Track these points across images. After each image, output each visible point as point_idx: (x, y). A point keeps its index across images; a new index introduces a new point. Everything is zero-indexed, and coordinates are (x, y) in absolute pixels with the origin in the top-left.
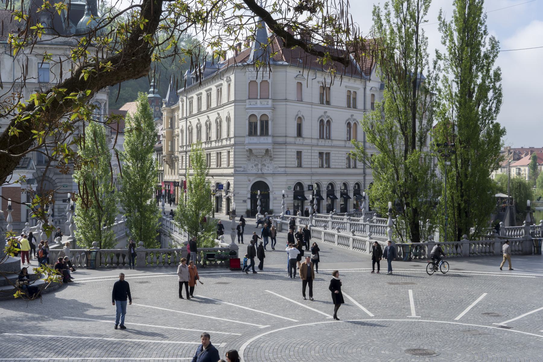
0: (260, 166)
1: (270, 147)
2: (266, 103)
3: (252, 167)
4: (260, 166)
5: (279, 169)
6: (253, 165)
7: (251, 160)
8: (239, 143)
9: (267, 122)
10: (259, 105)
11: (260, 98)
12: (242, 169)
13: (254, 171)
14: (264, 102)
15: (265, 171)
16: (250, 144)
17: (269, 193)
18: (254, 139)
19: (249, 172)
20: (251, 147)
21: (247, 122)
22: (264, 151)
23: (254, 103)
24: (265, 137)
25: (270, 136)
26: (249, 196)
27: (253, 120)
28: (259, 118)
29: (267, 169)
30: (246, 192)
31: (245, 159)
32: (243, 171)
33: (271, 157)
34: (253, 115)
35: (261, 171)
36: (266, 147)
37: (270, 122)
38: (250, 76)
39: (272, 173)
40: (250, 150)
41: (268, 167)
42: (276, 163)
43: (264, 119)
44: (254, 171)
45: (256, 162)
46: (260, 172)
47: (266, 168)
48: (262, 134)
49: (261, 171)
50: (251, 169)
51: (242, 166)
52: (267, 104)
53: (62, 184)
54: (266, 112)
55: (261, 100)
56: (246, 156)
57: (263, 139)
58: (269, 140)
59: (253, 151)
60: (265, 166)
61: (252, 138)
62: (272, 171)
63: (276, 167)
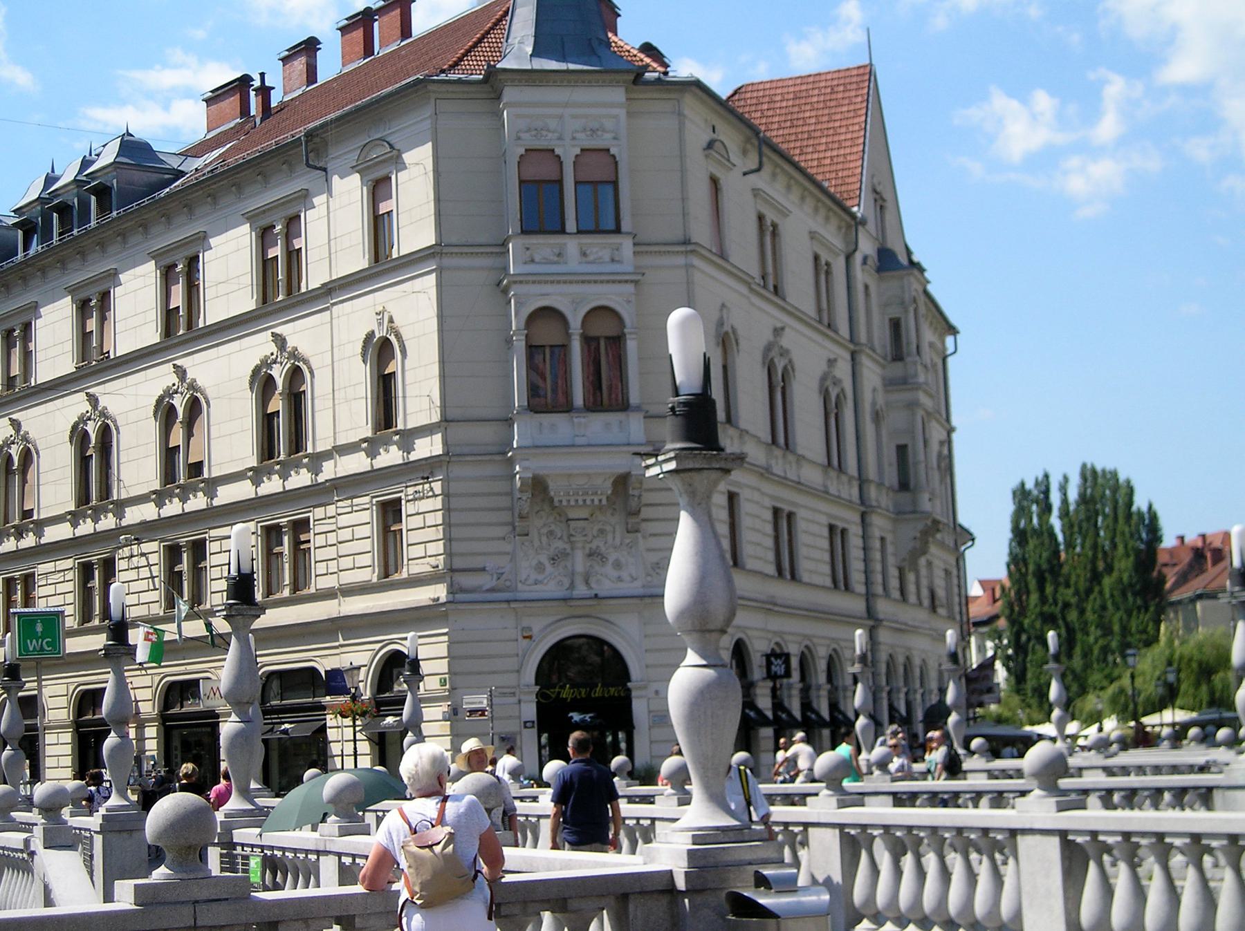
0: (579, 562)
2: (606, 254)
3: (540, 568)
4: (579, 562)
6: (544, 559)
7: (534, 533)
8: (466, 450)
9: (617, 341)
10: (573, 263)
11: (579, 232)
12: (485, 581)
14: (599, 246)
15: (605, 586)
17: (629, 690)
19: (525, 591)
24: (613, 418)
25: (638, 409)
26: (530, 711)
27: (548, 334)
29: (614, 574)
32: (492, 590)
34: (547, 313)
35: (587, 583)
37: (631, 346)
39: (640, 591)
41: (618, 565)
43: (603, 328)
44: (551, 588)
45: (560, 545)
46: (581, 590)
47: (609, 569)
48: (596, 404)
49: (587, 583)
50: (534, 576)
51: (490, 563)
52: (613, 260)
54: (612, 296)
55: (587, 240)
57: (598, 425)
59: (552, 486)
61: (547, 419)
62: (638, 584)
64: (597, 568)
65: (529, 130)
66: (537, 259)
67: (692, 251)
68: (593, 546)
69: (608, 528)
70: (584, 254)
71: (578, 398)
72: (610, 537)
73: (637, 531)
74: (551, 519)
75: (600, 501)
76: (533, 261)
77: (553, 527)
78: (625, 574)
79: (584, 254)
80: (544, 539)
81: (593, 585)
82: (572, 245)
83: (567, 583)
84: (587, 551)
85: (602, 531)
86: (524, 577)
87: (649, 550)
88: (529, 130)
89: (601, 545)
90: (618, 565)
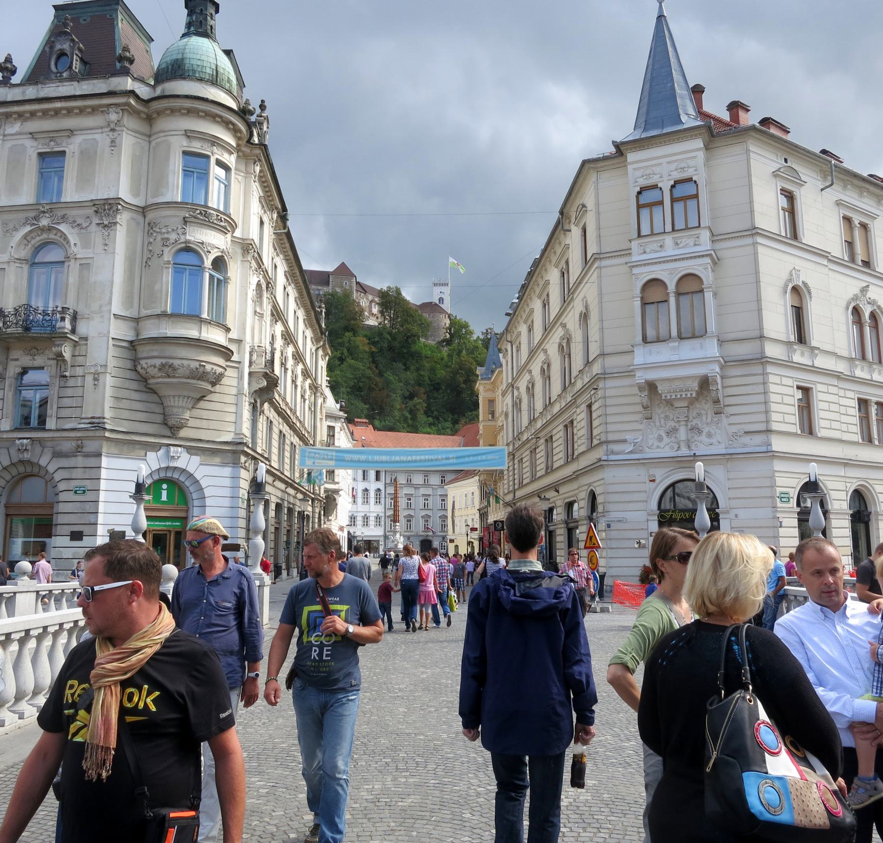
0: (682, 434)
1: (714, 370)
3: (660, 439)
4: (682, 434)
5: (746, 439)
10: (670, 250)
13: (667, 448)
14: (686, 238)
16: (647, 367)
18: (662, 353)
20: (652, 376)
21: (638, 303)
22: (695, 385)
23: (655, 246)
28: (671, 287)
30: (642, 516)
31: (638, 417)
33: (717, 401)
34: (654, 283)
35: (689, 447)
36: (701, 371)
38: (639, 173)
39: (724, 451)
40: (651, 387)
41: (709, 435)
42: (733, 419)
44: (667, 452)
45: (672, 424)
46: (684, 451)
47: (703, 438)
49: (689, 447)
50: (656, 443)
51: (628, 437)
52: (695, 245)
53: (73, 484)
56: (639, 408)
57: (688, 351)
58: (711, 348)
59: (660, 388)
60: (700, 432)
62: (723, 446)
63: (735, 434)
64: (696, 438)
65: (642, 176)
66: (648, 250)
67: (755, 234)
68: (694, 423)
69: (703, 412)
70: (677, 244)
71: (674, 333)
72: (704, 417)
73: (721, 413)
74: (666, 409)
75: (691, 394)
76: (645, 252)
77: (668, 413)
78: (714, 441)
79: (677, 244)
80: (663, 421)
81: (693, 447)
82: (668, 240)
83: (676, 446)
84: (689, 427)
85: (699, 415)
86: (650, 444)
87: (730, 424)
88: (642, 176)
89: (699, 423)
90: (709, 435)
